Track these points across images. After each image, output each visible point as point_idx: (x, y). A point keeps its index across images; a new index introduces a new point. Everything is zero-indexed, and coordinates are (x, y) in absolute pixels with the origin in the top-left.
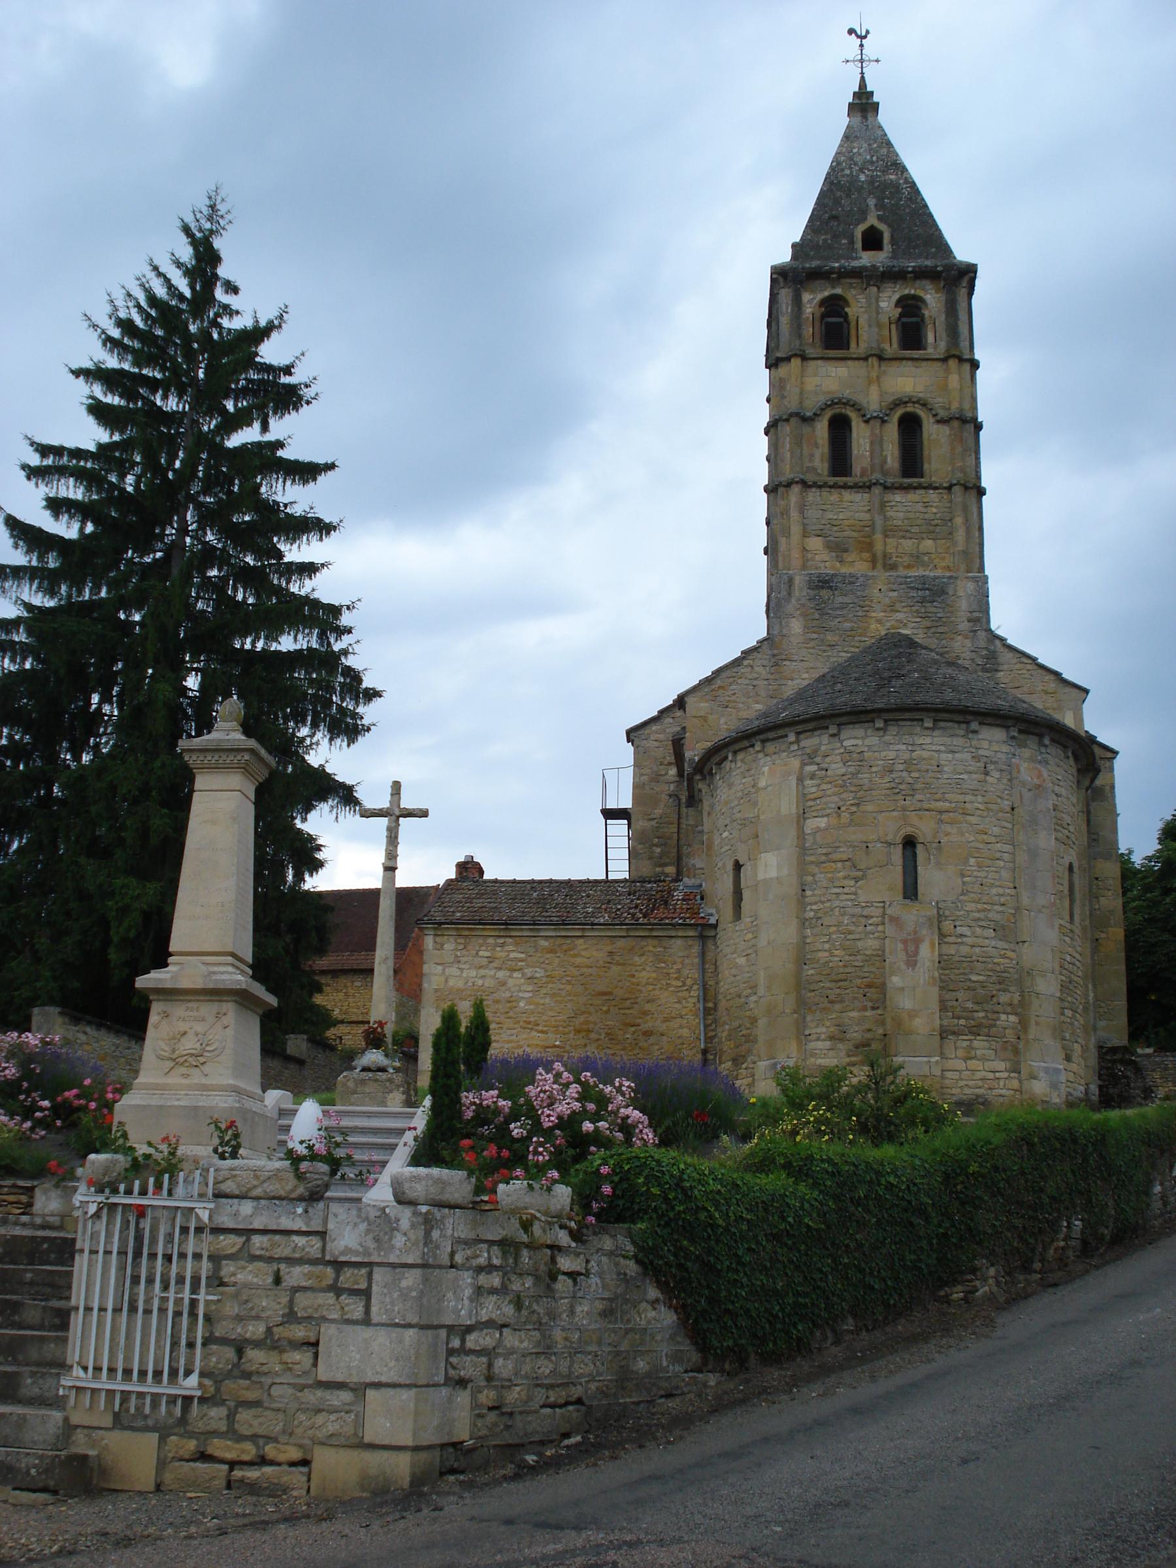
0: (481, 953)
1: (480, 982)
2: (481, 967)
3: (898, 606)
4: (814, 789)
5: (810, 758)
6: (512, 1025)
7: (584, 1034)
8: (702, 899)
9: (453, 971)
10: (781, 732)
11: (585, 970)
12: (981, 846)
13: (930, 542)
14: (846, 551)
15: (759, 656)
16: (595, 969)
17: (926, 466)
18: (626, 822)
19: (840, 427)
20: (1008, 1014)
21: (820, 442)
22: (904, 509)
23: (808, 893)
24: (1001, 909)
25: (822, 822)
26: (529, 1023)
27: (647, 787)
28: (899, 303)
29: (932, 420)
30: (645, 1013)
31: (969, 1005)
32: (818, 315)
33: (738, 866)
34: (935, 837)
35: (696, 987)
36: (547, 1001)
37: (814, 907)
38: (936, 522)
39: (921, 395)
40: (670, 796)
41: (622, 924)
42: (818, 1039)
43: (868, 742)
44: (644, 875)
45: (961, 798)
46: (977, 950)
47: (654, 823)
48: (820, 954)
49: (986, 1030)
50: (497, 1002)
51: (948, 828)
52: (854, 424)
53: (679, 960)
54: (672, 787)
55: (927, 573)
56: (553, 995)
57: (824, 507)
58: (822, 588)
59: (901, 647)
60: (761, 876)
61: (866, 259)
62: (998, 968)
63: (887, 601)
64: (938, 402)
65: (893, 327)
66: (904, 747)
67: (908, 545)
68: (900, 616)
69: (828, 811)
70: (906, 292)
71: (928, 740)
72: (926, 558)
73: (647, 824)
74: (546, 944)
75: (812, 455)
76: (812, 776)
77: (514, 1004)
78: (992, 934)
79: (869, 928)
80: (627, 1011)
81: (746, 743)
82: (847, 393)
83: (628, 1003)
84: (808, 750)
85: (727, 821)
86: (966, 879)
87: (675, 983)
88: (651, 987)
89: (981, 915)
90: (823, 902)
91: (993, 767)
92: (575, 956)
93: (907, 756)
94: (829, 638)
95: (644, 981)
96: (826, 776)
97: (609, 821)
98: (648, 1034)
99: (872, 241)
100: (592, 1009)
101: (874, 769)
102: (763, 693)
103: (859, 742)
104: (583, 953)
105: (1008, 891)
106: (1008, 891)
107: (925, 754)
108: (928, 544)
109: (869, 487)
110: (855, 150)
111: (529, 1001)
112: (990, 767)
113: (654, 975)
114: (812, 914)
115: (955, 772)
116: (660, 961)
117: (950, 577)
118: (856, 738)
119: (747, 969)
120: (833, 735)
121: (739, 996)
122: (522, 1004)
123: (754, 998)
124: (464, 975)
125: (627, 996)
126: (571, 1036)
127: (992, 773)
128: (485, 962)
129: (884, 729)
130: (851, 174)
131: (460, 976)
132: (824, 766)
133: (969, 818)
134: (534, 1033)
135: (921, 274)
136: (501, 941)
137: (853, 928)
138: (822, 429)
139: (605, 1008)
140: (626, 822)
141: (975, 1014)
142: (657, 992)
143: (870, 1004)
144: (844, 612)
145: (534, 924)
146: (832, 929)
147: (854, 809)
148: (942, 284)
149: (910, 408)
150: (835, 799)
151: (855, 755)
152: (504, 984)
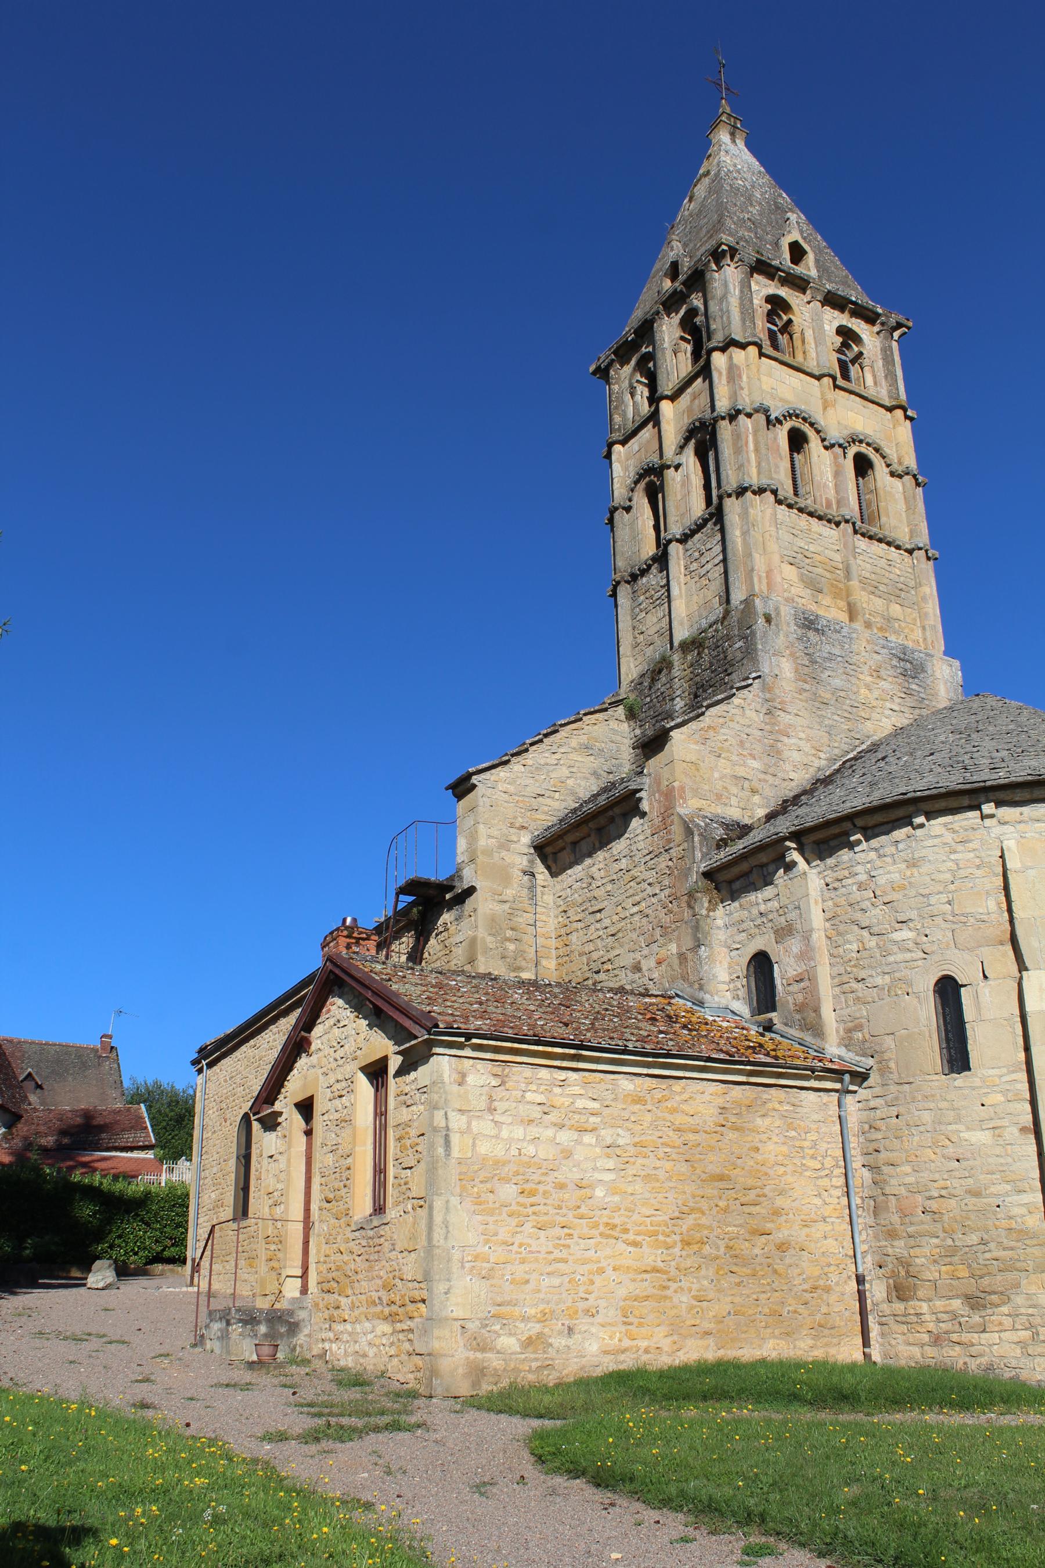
0: (529, 1096)
1: (531, 1150)
2: (531, 1121)
3: (883, 673)
6: (586, 1230)
7: (696, 1247)
9: (483, 1126)
11: (691, 1136)
15: (751, 696)
22: (871, 561)
26: (614, 1227)
29: (887, 470)
30: (777, 1213)
36: (638, 1186)
38: (901, 586)
47: (508, 905)
50: (561, 1186)
53: (813, 1126)
54: (525, 863)
56: (647, 1178)
74: (631, 1087)
77: (588, 1192)
81: (966, 801)
83: (752, 1194)
88: (783, 1169)
92: (673, 1111)
95: (772, 1158)
98: (782, 1247)
100: (704, 1205)
102: (758, 748)
104: (684, 1107)
108: (896, 609)
109: (838, 524)
111: (613, 1190)
113: (785, 1149)
116: (790, 1127)
119: (998, 1151)
122: (599, 1192)
124: (505, 1134)
125: (750, 1182)
126: (677, 1251)
131: (497, 1137)
134: (621, 1246)
136: (563, 1075)
145: (625, 1052)
148: (877, 328)
149: (863, 449)
152: (568, 1154)
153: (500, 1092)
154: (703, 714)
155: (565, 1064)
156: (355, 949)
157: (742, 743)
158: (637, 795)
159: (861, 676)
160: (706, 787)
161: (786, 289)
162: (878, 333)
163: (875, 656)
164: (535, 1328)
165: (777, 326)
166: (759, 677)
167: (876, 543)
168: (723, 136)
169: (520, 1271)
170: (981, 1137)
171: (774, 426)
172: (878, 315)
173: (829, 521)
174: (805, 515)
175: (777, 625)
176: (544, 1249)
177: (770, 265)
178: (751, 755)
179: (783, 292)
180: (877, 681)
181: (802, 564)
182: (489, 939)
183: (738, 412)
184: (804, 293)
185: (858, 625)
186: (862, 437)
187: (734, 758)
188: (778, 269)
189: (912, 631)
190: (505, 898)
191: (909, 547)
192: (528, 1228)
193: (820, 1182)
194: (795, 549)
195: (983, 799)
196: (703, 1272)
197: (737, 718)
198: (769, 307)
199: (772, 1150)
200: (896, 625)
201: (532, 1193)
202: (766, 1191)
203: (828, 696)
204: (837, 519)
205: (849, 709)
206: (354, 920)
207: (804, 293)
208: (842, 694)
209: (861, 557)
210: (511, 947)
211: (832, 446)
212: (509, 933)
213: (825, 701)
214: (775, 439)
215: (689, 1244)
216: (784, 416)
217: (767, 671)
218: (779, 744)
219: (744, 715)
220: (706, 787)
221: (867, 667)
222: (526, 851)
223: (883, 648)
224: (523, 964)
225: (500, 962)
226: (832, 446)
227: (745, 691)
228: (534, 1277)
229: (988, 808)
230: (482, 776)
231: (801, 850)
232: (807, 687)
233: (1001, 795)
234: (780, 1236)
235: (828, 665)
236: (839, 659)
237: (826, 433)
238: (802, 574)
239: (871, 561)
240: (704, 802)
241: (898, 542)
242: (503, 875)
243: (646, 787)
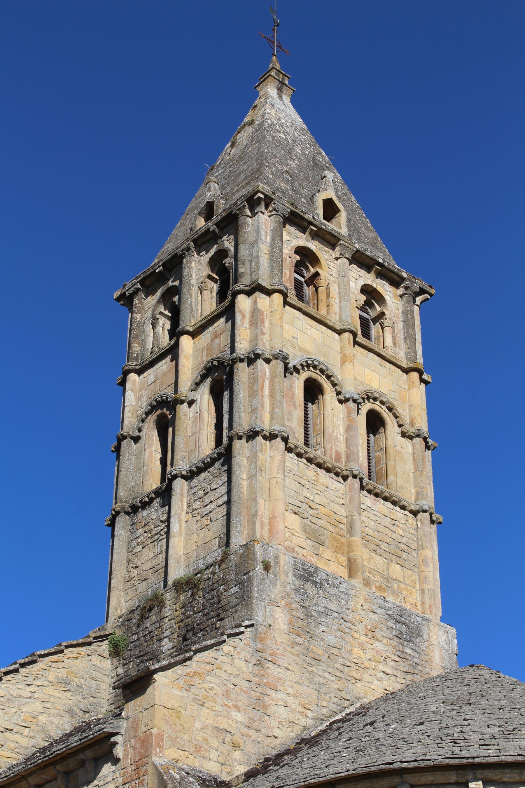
3: (378, 633)
15: (241, 644)
22: (375, 518)
29: (398, 430)
68: (377, 645)
108: (396, 570)
109: (345, 478)
144: (328, 620)
149: (377, 407)
154: (190, 658)
157: (227, 693)
158: (112, 739)
159: (356, 635)
160: (186, 737)
161: (316, 243)
162: (401, 296)
163: (372, 615)
165: (304, 277)
166: (252, 625)
167: (381, 500)
171: (292, 374)
172: (403, 279)
173: (337, 474)
174: (313, 466)
175: (275, 574)
177: (303, 219)
178: (235, 706)
179: (314, 246)
180: (371, 641)
181: (306, 515)
183: (258, 356)
184: (333, 249)
185: (357, 582)
186: (376, 395)
187: (218, 708)
188: (311, 223)
189: (411, 593)
191: (414, 508)
195: (471, 777)
197: (226, 667)
198: (298, 258)
200: (395, 586)
203: (321, 652)
204: (345, 473)
205: (341, 668)
207: (333, 249)
208: (335, 651)
211: (347, 400)
213: (317, 657)
214: (291, 387)
216: (302, 365)
217: (260, 620)
218: (266, 698)
220: (186, 737)
221: (362, 626)
223: (380, 607)
226: (347, 400)
227: (236, 639)
232: (300, 640)
233: (490, 774)
235: (324, 620)
236: (335, 615)
237: (342, 387)
238: (305, 525)
239: (375, 518)
240: (182, 753)
241: (403, 503)
243: (122, 731)
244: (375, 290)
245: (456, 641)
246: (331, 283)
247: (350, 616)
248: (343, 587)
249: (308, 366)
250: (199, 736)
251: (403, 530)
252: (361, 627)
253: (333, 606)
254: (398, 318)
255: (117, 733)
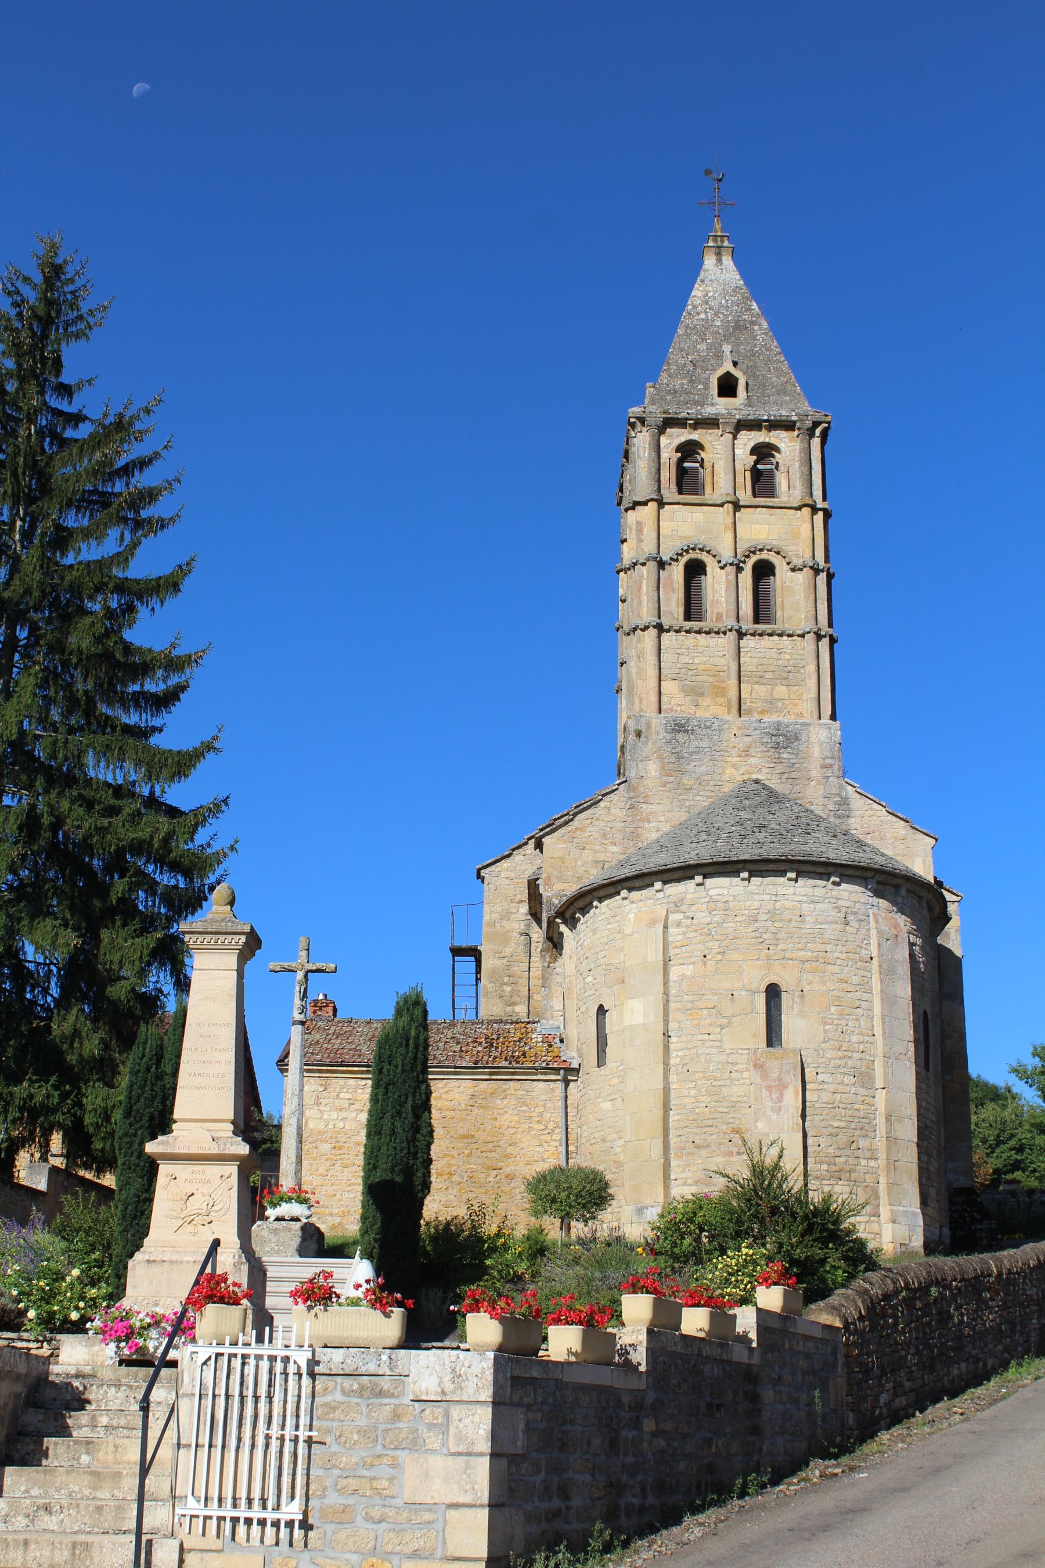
0: (342, 1095)
2: (341, 1110)
3: (752, 751)
4: (680, 937)
5: (677, 905)
8: (562, 1041)
10: (647, 881)
12: (841, 995)
13: (784, 688)
14: (701, 695)
16: (458, 1112)
17: (779, 613)
18: (473, 959)
19: (695, 570)
20: (868, 1159)
21: (676, 586)
23: (673, 1039)
24: (862, 1055)
25: (689, 970)
27: (498, 925)
28: (754, 451)
30: (507, 1156)
31: (831, 1150)
32: (674, 460)
33: (601, 1011)
34: (797, 986)
35: (557, 1131)
37: (680, 1053)
38: (789, 668)
39: (775, 543)
40: (521, 934)
41: (485, 1068)
42: (684, 1184)
43: (732, 891)
44: (495, 1014)
45: (823, 947)
46: (838, 1096)
48: (686, 1100)
49: (848, 1175)
51: (810, 977)
52: (708, 569)
54: (523, 926)
55: (781, 719)
57: (680, 651)
58: (679, 731)
59: (760, 795)
60: (627, 1022)
61: (721, 406)
62: (857, 1114)
63: (741, 746)
64: (791, 550)
65: (748, 474)
66: (768, 897)
67: (761, 690)
69: (694, 959)
70: (761, 440)
71: (791, 890)
72: (780, 705)
73: (498, 963)
75: (668, 599)
76: (678, 925)
78: (853, 1080)
79: (734, 1075)
80: (489, 1154)
82: (702, 540)
83: (490, 1145)
84: (674, 899)
85: (592, 966)
86: (827, 1027)
87: (536, 1126)
89: (842, 1062)
90: (689, 1049)
91: (852, 917)
93: (770, 907)
94: (685, 782)
95: (506, 1123)
96: (692, 924)
97: (456, 958)
99: (727, 387)
100: (455, 1152)
101: (738, 919)
102: (619, 837)
103: (725, 892)
105: (867, 1038)
106: (867, 1038)
107: (788, 904)
108: (781, 691)
109: (725, 633)
110: (710, 294)
112: (850, 918)
113: (516, 1118)
114: (678, 1060)
115: (816, 922)
117: (803, 724)
118: (720, 886)
120: (698, 885)
121: (604, 1141)
123: (621, 1142)
124: (325, 1117)
125: (489, 1139)
127: (852, 923)
128: (346, 1104)
129: (749, 880)
130: (706, 320)
131: (321, 1118)
132: (690, 914)
133: (829, 967)
135: (774, 425)
137: (718, 1075)
138: (677, 573)
139: (467, 1152)
140: (473, 959)
141: (837, 1159)
142: (519, 1136)
143: (736, 1150)
144: (700, 756)
146: (698, 1076)
147: (719, 957)
149: (764, 555)
150: (701, 947)
151: (720, 904)
153: (325, 1094)
154: (572, 820)
155: (364, 1076)
156: (319, 1013)
159: (728, 759)
161: (700, 431)
163: (746, 739)
164: (337, 1220)
166: (626, 781)
168: (709, 261)
169: (331, 1190)
170: (607, 1105)
171: (670, 564)
172: (795, 422)
173: (717, 633)
175: (647, 737)
176: (345, 1178)
177: (678, 419)
179: (695, 435)
181: (685, 677)
182: (491, 985)
183: (635, 564)
187: (597, 847)
188: (687, 419)
190: (503, 954)
191: (800, 632)
192: (337, 1167)
193: (542, 1138)
194: (679, 666)
196: (450, 1191)
197: (603, 817)
198: (679, 455)
199: (508, 1118)
200: (780, 705)
201: (340, 1148)
202: (500, 1143)
203: (691, 783)
204: (723, 630)
206: (325, 995)
209: (749, 654)
210: (508, 989)
211: (725, 565)
212: (506, 979)
214: (670, 576)
215: (441, 1175)
216: (677, 554)
219: (609, 813)
220: (570, 874)
222: (523, 918)
223: (756, 729)
224: (518, 999)
225: (498, 1001)
226: (725, 565)
227: (612, 795)
228: (339, 1194)
229: (624, 893)
230: (489, 869)
231: (565, 922)
232: (671, 779)
234: (507, 1170)
242: (504, 938)
244: (769, 443)
245: (839, 733)
246: (716, 461)
247: (723, 746)
248: (715, 726)
249: (681, 555)
250: (581, 870)
251: (790, 654)
252: (734, 752)
253: (704, 744)
254: (793, 460)
255: (538, 879)
